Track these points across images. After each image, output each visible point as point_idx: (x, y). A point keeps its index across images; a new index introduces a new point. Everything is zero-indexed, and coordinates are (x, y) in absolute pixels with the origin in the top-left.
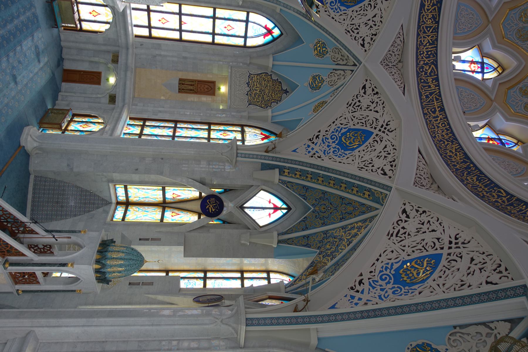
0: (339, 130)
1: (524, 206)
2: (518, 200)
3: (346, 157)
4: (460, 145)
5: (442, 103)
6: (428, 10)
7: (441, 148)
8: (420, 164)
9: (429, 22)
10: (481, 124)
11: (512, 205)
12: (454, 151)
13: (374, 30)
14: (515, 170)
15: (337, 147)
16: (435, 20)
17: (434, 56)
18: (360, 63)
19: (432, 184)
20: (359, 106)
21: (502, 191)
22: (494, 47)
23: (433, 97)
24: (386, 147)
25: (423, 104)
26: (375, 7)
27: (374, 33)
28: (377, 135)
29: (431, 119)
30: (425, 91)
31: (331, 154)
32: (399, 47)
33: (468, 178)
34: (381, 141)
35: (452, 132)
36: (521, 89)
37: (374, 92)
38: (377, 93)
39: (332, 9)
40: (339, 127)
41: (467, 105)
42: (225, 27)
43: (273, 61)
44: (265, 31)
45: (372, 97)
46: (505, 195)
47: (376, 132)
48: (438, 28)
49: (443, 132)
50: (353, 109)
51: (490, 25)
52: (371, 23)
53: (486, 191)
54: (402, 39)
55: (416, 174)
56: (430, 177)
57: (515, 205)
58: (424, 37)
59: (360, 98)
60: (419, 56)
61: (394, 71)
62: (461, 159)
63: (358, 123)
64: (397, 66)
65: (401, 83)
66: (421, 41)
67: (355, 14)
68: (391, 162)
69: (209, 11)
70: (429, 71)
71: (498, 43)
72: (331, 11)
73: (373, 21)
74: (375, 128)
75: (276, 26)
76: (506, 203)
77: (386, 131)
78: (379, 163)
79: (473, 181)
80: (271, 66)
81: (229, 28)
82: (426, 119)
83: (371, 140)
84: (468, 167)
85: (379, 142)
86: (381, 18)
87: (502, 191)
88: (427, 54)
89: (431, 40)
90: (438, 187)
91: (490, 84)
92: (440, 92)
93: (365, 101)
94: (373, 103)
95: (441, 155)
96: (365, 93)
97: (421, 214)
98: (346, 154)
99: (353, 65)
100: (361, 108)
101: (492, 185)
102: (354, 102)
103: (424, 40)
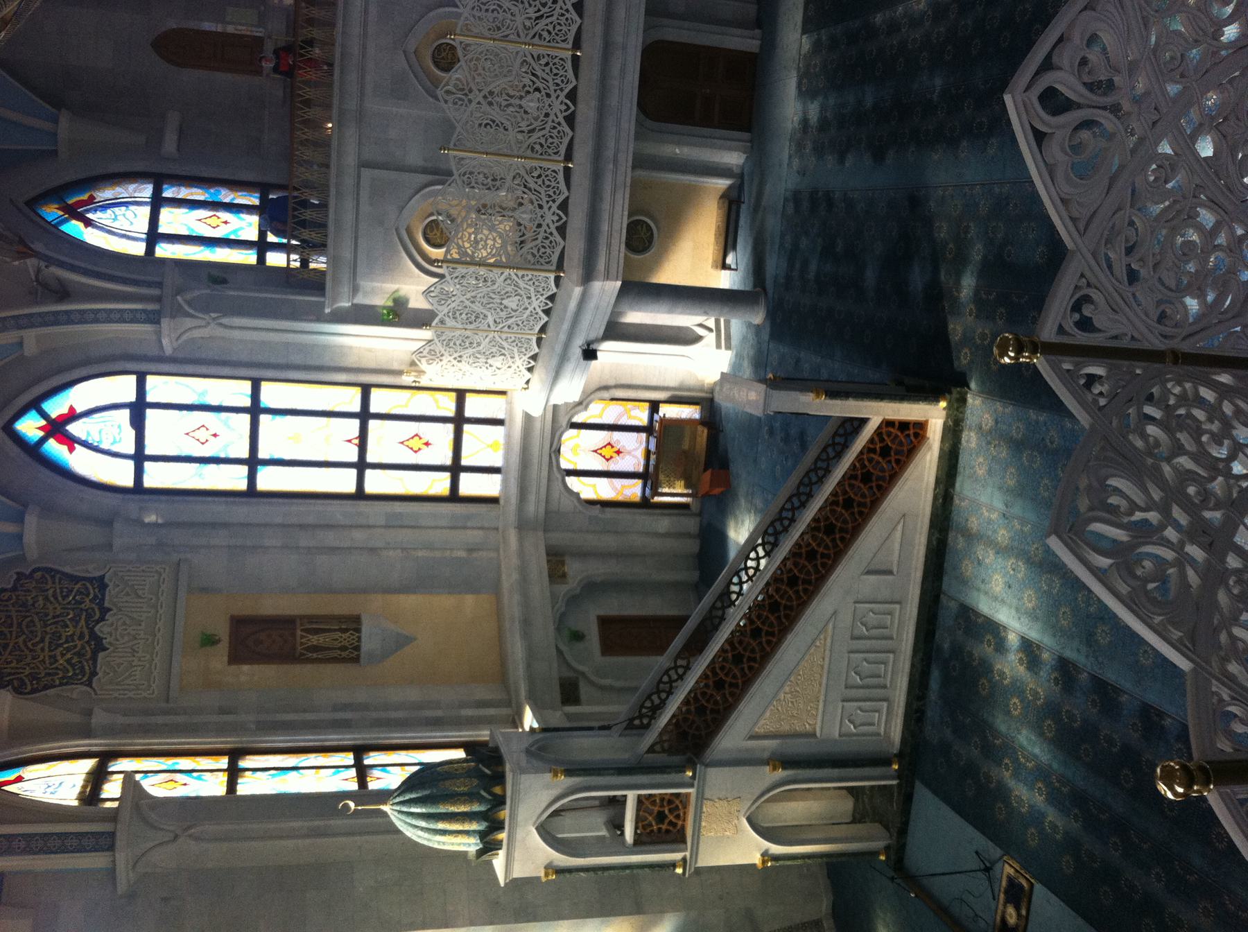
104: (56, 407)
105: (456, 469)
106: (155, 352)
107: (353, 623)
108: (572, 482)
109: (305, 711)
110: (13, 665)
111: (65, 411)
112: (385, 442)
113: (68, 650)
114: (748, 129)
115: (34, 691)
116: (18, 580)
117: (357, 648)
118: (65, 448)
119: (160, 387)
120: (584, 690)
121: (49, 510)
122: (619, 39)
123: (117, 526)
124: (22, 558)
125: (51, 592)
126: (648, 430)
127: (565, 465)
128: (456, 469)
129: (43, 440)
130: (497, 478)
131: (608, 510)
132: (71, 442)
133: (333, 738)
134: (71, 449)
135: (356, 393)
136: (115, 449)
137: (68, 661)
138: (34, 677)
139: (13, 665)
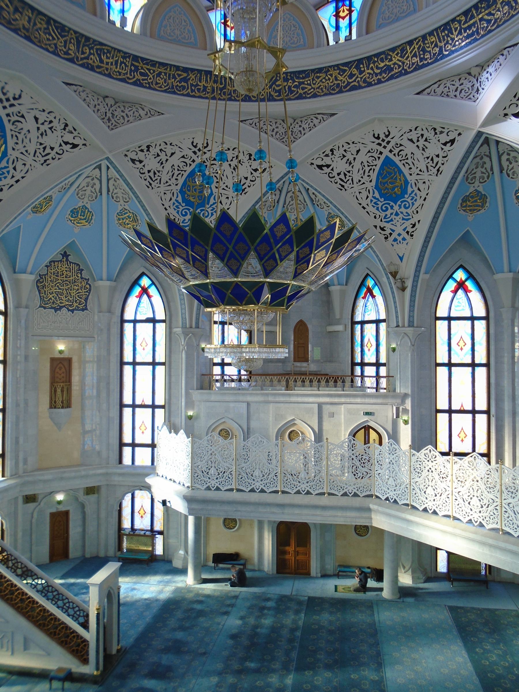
13: (429, 135)
26: (401, 145)
27: (433, 133)
39: (413, 204)
42: (462, 349)
43: (503, 272)
44: (460, 292)
52: (421, 143)
67: (414, 169)
69: (442, 373)
72: (416, 204)
73: (418, 141)
75: (451, 277)
80: (511, 275)
81: (461, 344)
86: (411, 130)
104: (153, 291)
105: (134, 445)
106: (173, 325)
107: (67, 404)
108: (128, 497)
109: (25, 388)
110: (49, 279)
111: (151, 294)
112: (143, 416)
113: (56, 298)
114: (278, 572)
115: (38, 287)
116: (86, 279)
117: (55, 407)
118: (137, 294)
119: (161, 328)
120: (32, 506)
121: (113, 290)
122: (287, 510)
123: (107, 314)
124: (94, 280)
125: (80, 291)
126: (152, 530)
127: (137, 493)
128: (134, 445)
129: (140, 286)
130: (130, 463)
131: (117, 513)
132: (140, 296)
133: (9, 400)
134: (137, 297)
135: (163, 403)
136: (138, 313)
137: (51, 299)
138: (44, 286)
139: (49, 279)
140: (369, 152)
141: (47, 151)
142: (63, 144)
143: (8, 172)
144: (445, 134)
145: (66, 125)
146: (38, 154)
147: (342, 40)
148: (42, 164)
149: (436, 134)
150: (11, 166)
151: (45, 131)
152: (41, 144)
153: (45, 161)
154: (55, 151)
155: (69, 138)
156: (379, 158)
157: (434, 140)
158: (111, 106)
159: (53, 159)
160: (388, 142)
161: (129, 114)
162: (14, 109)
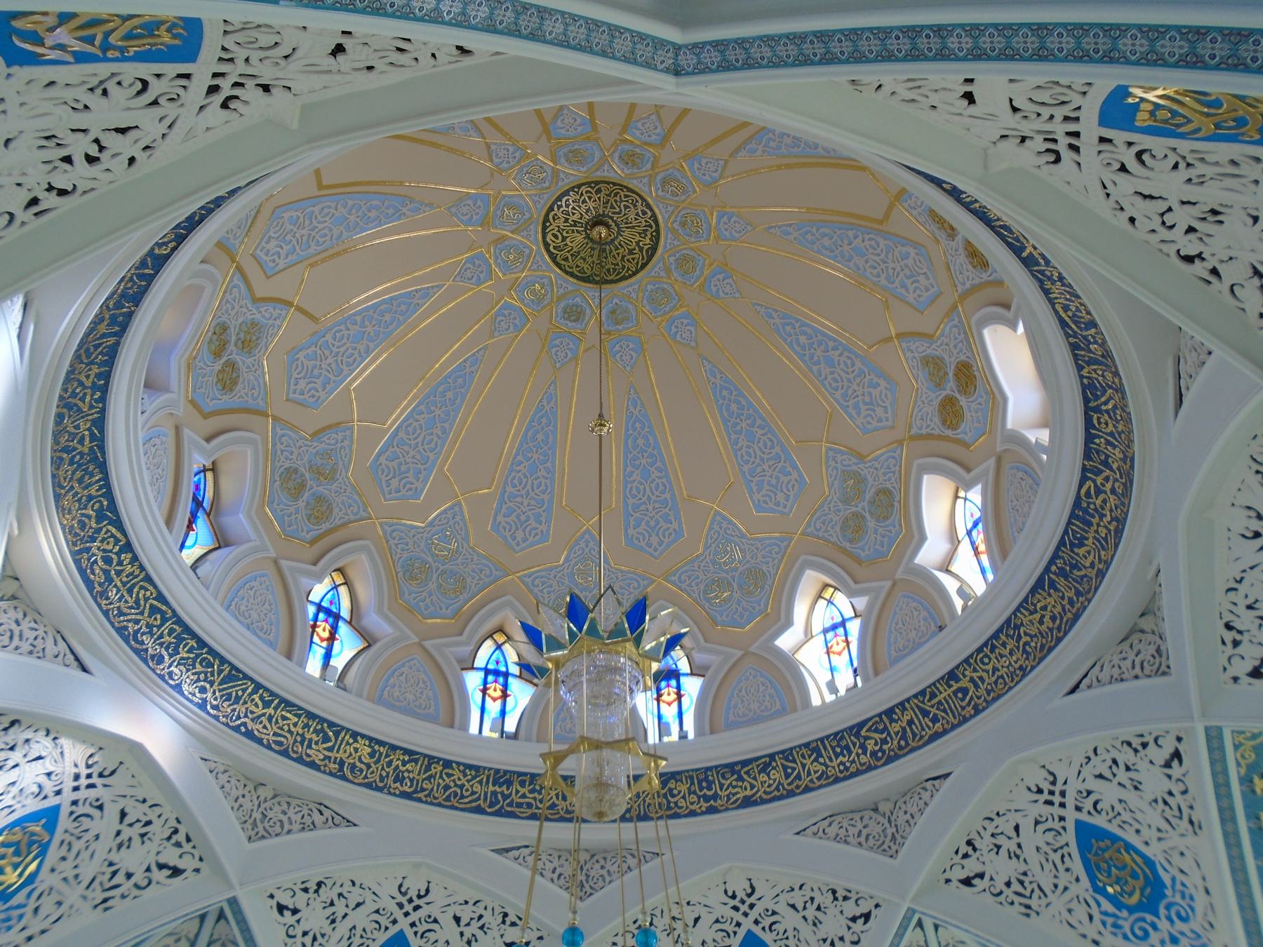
0: (1110, 920)
1: (1097, 441)
2: (1087, 455)
3: (1179, 877)
4: (1018, 609)
5: (938, 681)
6: (752, 787)
7: (1043, 646)
8: (1104, 676)
9: (775, 775)
10: (951, 585)
11: (1106, 463)
12: (1037, 616)
14: (1023, 483)
15: (1162, 911)
16: (770, 763)
17: (842, 738)
18: (911, 912)
19: (1142, 631)
20: (1022, 883)
21: (1083, 491)
22: (789, 623)
23: (932, 706)
24: (1101, 776)
25: (956, 722)
26: (774, 913)
27: (830, 895)
28: (1078, 809)
29: (982, 692)
30: (923, 729)
31: (1195, 925)
32: (845, 824)
33: (1088, 564)
34: (1089, 793)
35: (995, 636)
36: (851, 541)
37: (971, 852)
38: (969, 843)
40: (1104, 924)
41: (924, 628)
45: (985, 851)
46: (1089, 483)
47: (1071, 815)
48: (782, 752)
49: (1002, 656)
50: (1035, 895)
51: (753, 649)
52: (811, 912)
53: (1101, 519)
54: (826, 822)
55: (1136, 677)
56: (1128, 643)
57: (1103, 457)
58: (809, 774)
59: (1000, 885)
60: (852, 770)
61: (902, 819)
62: (1050, 595)
63: (1067, 870)
64: (888, 813)
65: (925, 789)
66: (819, 779)
68: (1136, 751)
70: (877, 736)
71: (779, 619)
73: (805, 908)
74: (1062, 819)
76: (1108, 472)
77: (1057, 789)
78: (1154, 781)
79: (1089, 552)
82: (989, 703)
83: (1099, 821)
84: (1062, 573)
85: (1093, 798)
86: (793, 890)
87: (1083, 491)
88: (842, 754)
89: (810, 756)
90: (1142, 615)
91: (861, 602)
92: (915, 696)
93: (1002, 869)
94: (998, 847)
95: (1059, 640)
96: (981, 876)
97: (1240, 632)
98: (1173, 879)
99: (922, 928)
100: (1025, 874)
101: (1080, 513)
102: (1017, 899)
103: (816, 772)
140: (717, 921)
141: (115, 881)
142: (154, 868)
143: (21, 917)
144: (852, 901)
145: (176, 831)
146: (96, 883)
147: (675, 737)
148: (96, 906)
149: (836, 899)
150: (32, 904)
151: (130, 839)
152: (111, 864)
153: (105, 901)
154: (133, 880)
155: (171, 856)
156: (735, 933)
157: (832, 910)
158: (265, 801)
159: (123, 897)
160: (752, 906)
161: (294, 817)
162: (92, 794)
